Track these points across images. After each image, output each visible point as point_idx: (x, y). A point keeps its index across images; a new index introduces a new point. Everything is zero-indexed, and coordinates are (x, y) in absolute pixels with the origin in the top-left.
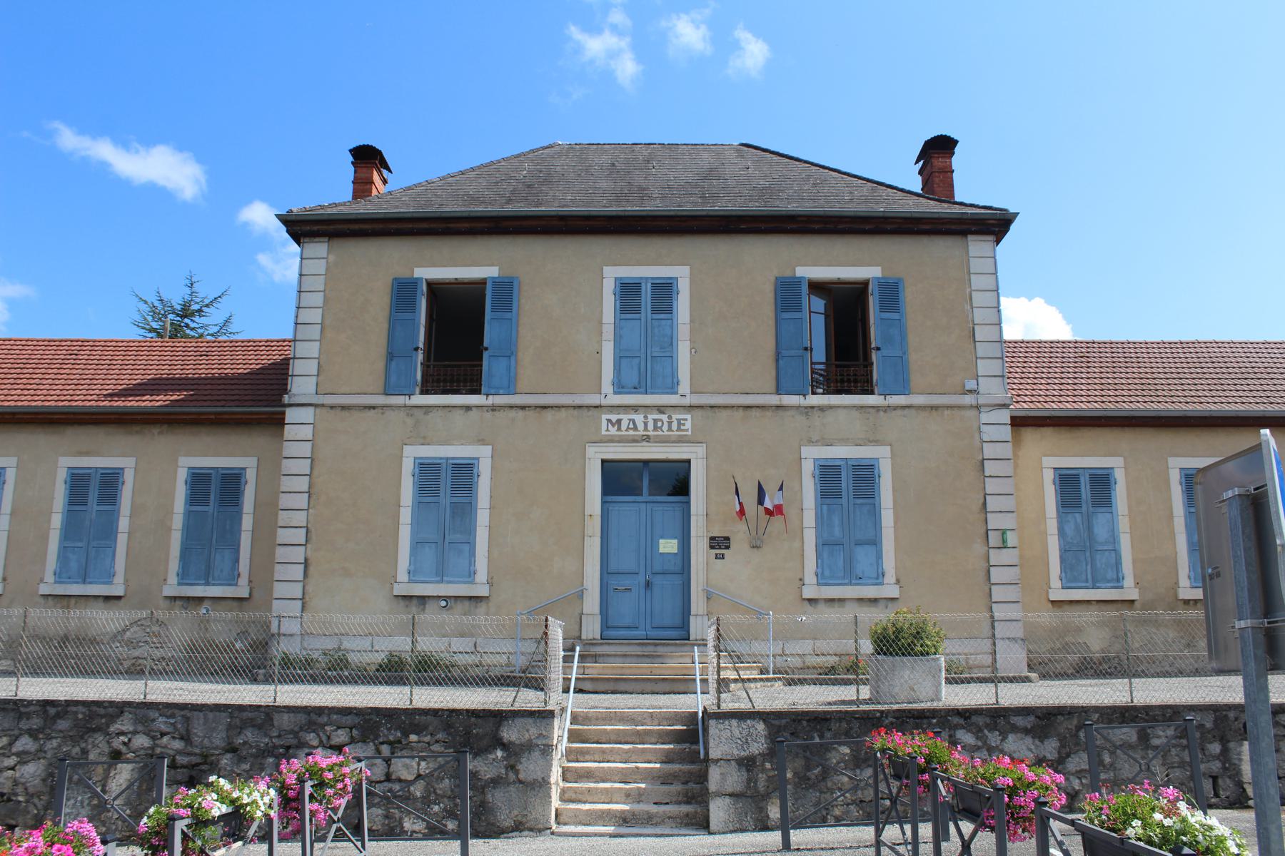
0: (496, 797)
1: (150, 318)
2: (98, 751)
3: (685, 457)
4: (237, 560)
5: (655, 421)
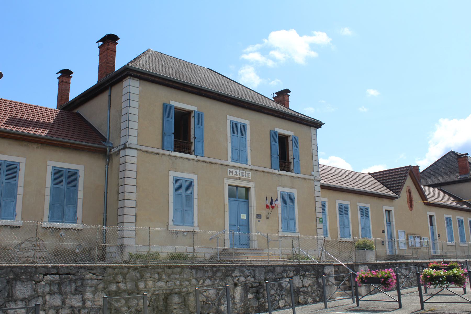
4: (76, 212)
5: (242, 173)
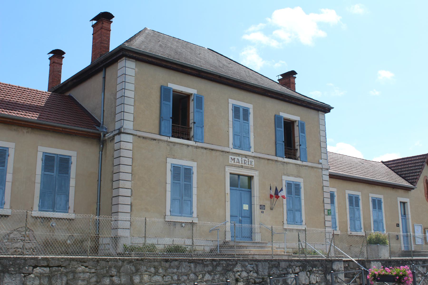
2: (231, 279)
3: (252, 175)
4: (68, 201)
5: (245, 160)
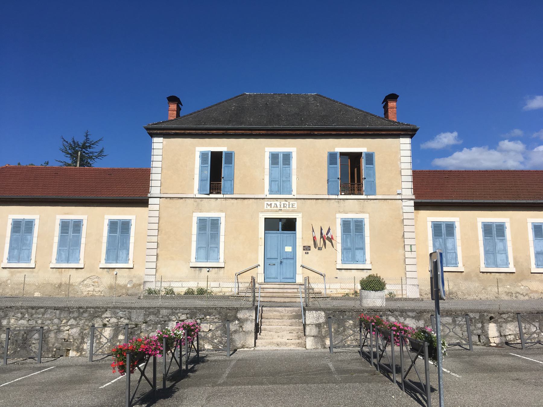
0: (236, 337)
1: (68, 148)
